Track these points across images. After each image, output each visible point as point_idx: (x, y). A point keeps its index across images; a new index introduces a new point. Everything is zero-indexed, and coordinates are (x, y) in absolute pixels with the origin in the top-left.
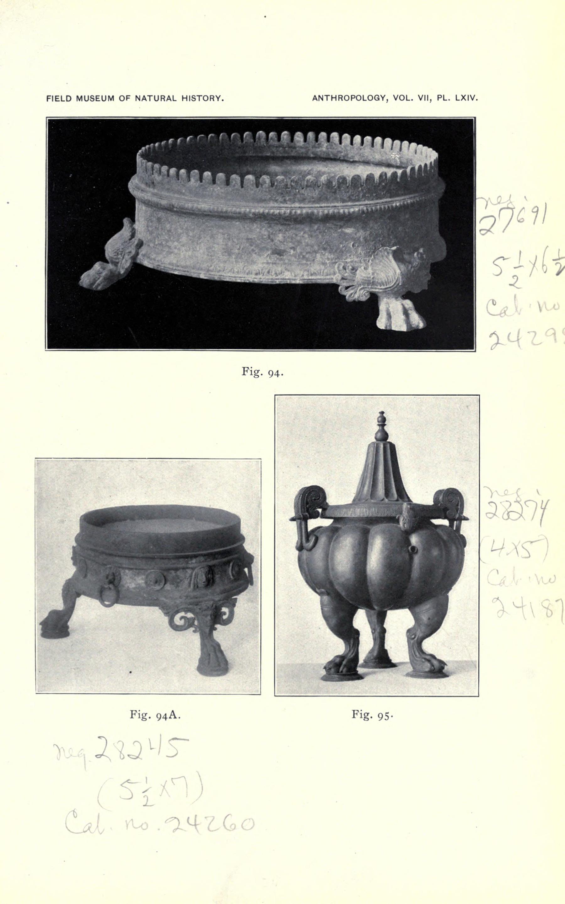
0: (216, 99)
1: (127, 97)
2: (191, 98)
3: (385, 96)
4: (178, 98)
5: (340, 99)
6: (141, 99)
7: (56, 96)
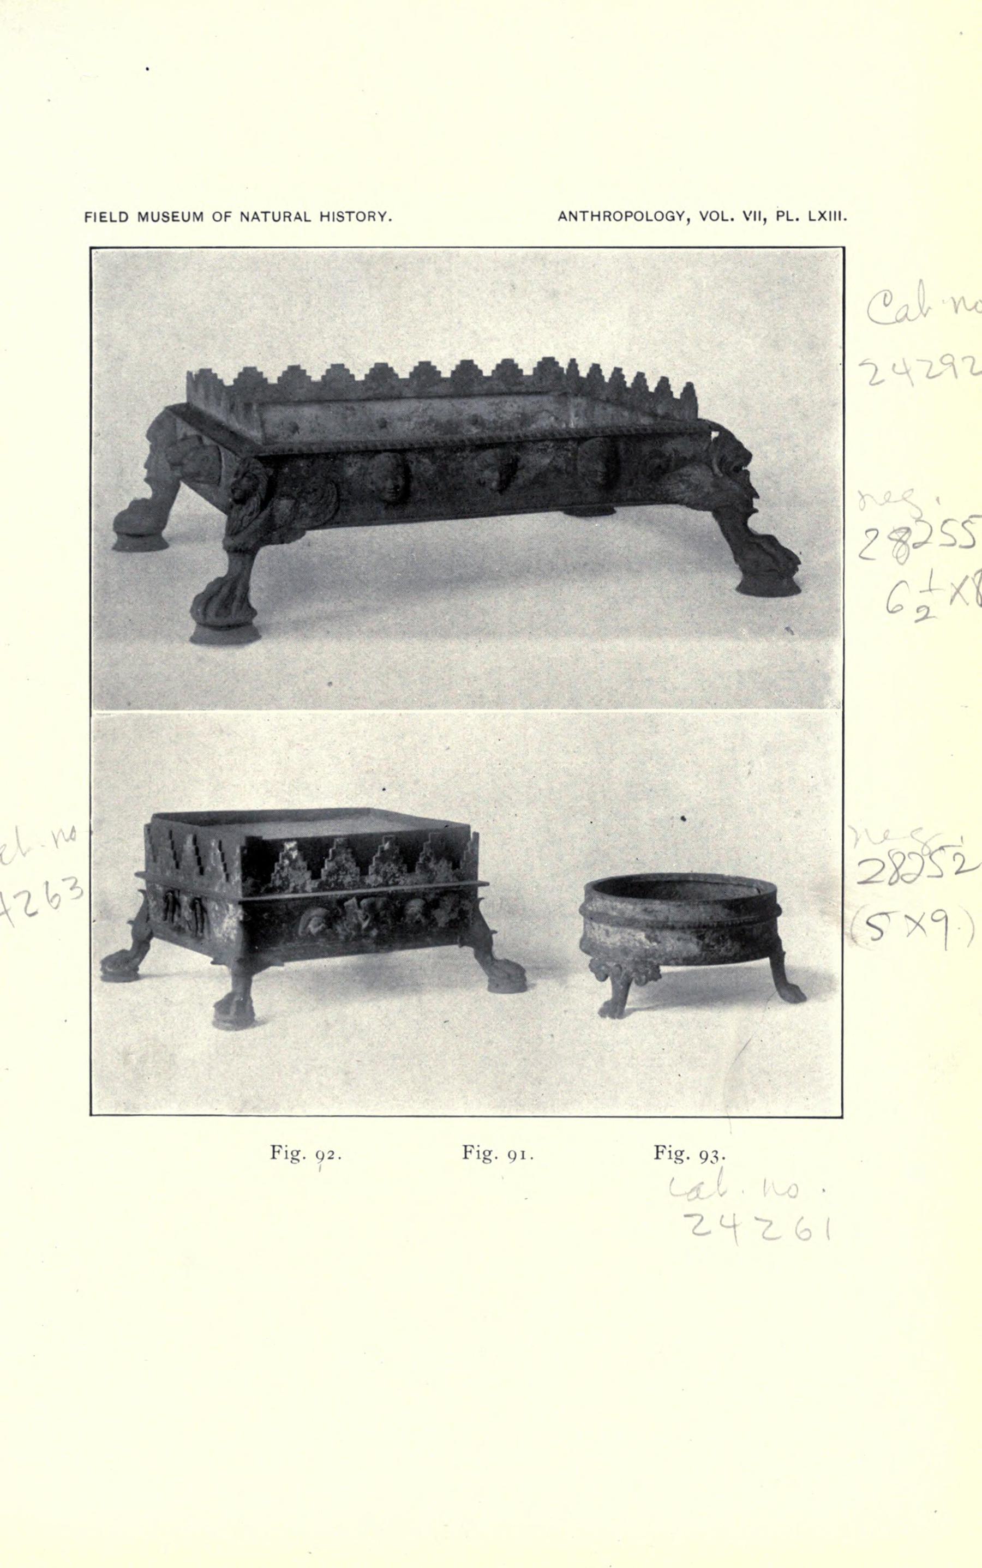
0: (378, 217)
2: (336, 216)
4: (314, 216)
5: (607, 218)
6: (250, 218)
7: (101, 213)
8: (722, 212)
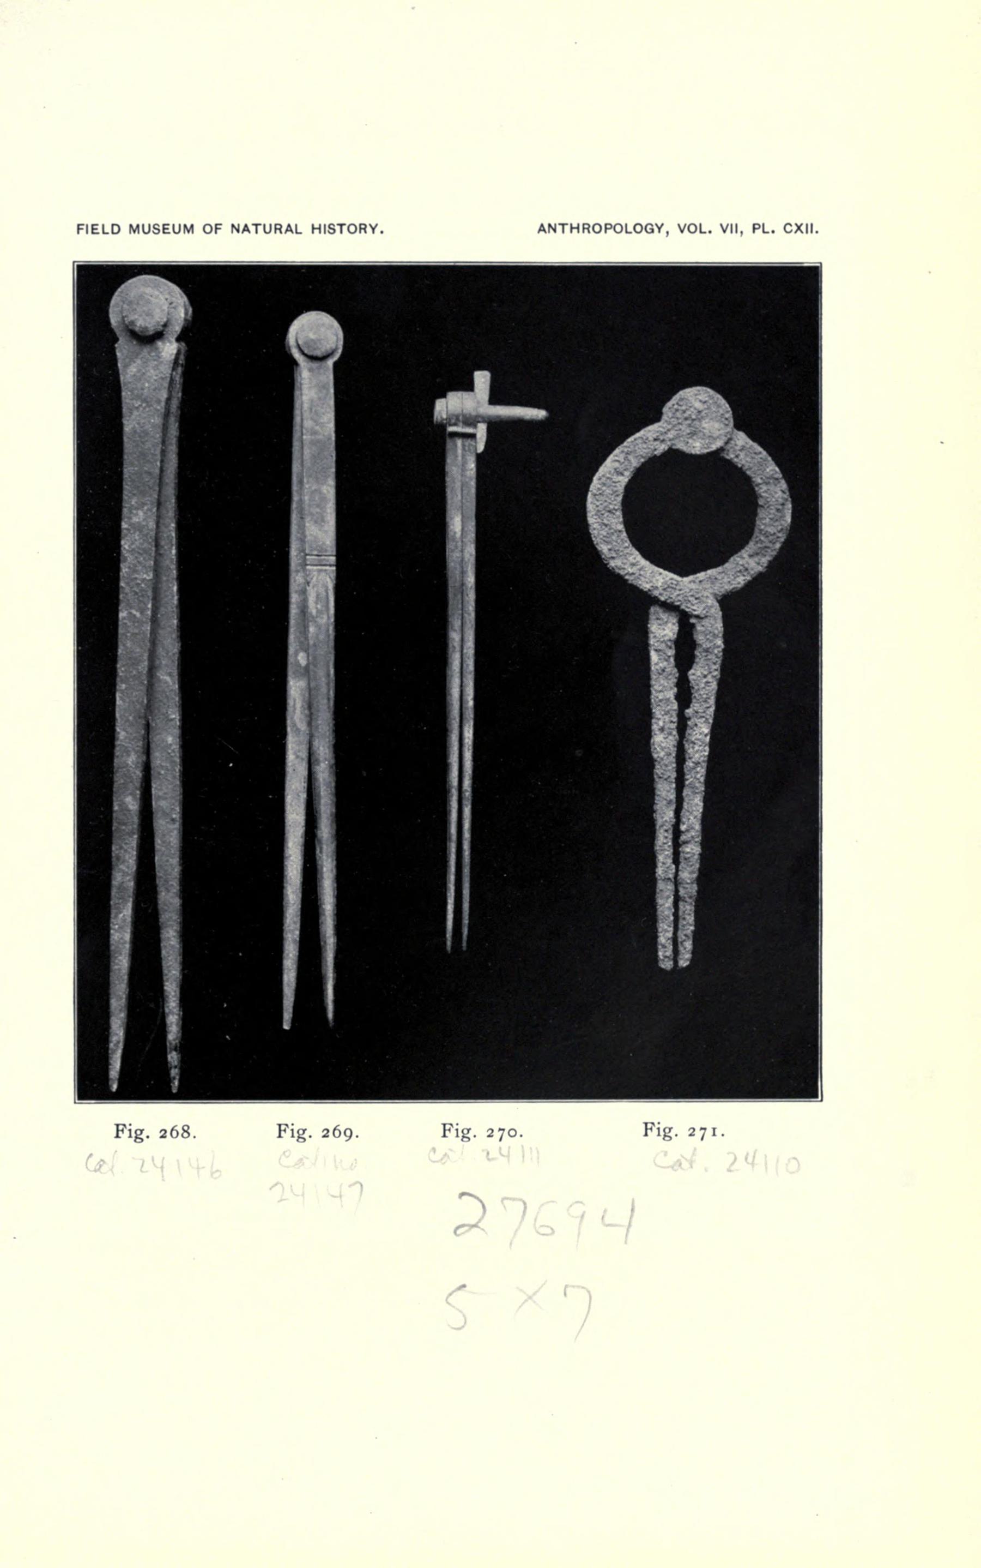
0: (369, 229)
1: (217, 227)
2: (327, 228)
3: (662, 225)
4: (305, 228)
5: (586, 231)
6: (241, 229)
7: (93, 225)
8: (700, 225)
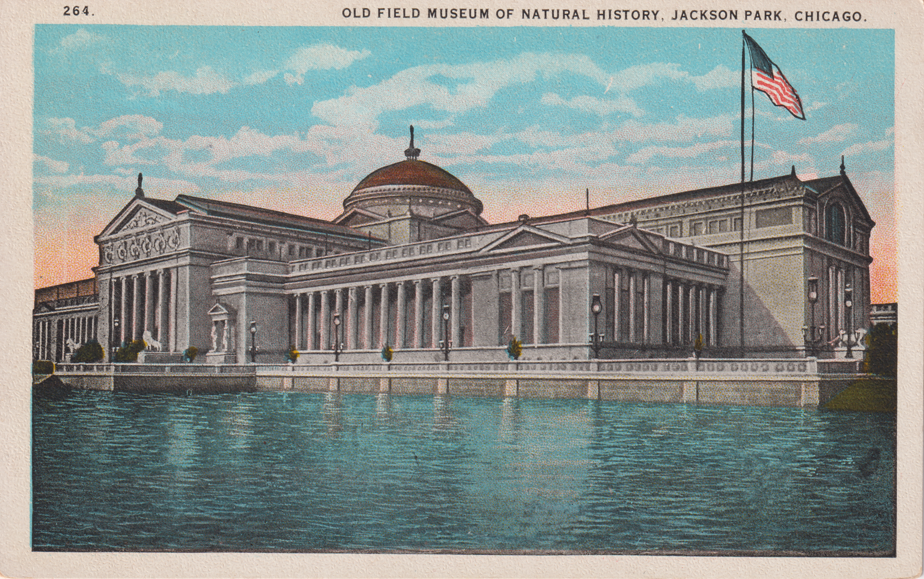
0: (651, 16)
2: (613, 13)
4: (592, 13)
6: (531, 15)
